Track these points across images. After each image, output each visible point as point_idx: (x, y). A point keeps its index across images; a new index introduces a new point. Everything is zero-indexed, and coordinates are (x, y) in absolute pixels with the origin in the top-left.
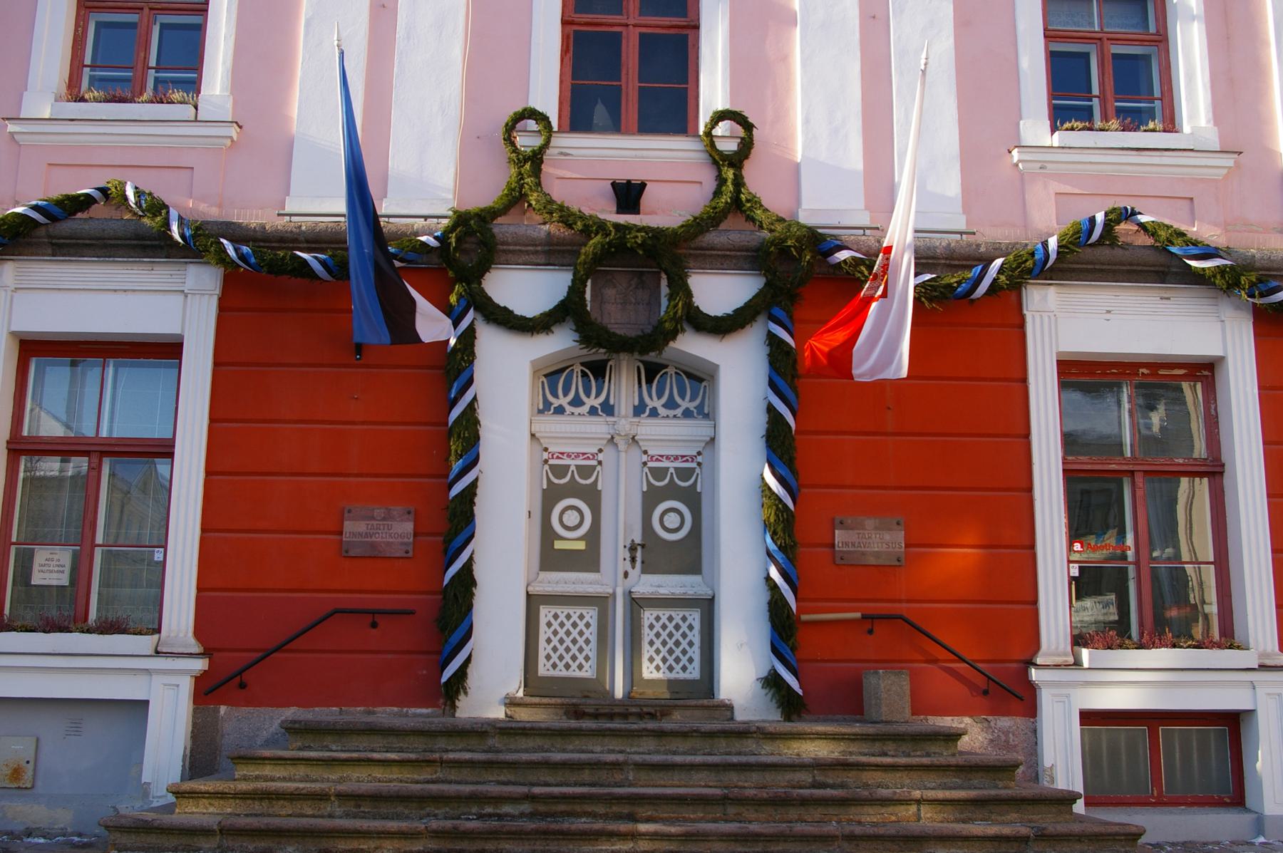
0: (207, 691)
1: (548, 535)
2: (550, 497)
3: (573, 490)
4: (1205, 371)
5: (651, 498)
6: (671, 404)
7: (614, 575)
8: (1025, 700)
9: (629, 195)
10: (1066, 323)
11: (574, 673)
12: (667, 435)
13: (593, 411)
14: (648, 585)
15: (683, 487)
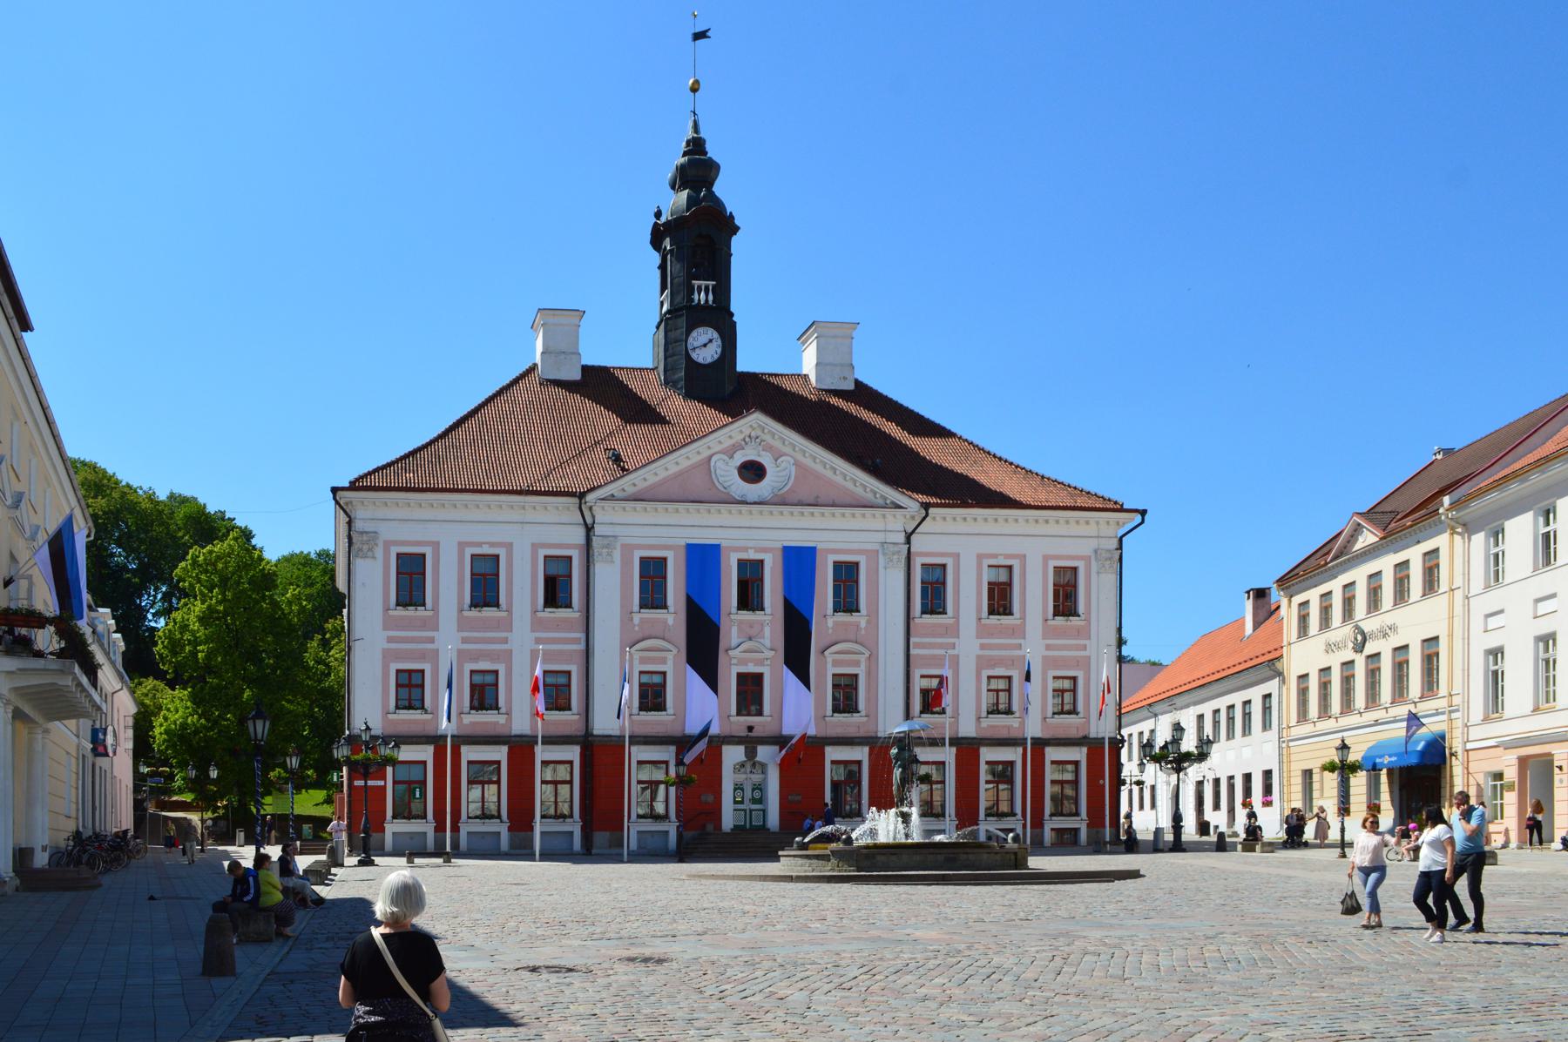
9: (750, 729)
10: (832, 754)
15: (760, 788)
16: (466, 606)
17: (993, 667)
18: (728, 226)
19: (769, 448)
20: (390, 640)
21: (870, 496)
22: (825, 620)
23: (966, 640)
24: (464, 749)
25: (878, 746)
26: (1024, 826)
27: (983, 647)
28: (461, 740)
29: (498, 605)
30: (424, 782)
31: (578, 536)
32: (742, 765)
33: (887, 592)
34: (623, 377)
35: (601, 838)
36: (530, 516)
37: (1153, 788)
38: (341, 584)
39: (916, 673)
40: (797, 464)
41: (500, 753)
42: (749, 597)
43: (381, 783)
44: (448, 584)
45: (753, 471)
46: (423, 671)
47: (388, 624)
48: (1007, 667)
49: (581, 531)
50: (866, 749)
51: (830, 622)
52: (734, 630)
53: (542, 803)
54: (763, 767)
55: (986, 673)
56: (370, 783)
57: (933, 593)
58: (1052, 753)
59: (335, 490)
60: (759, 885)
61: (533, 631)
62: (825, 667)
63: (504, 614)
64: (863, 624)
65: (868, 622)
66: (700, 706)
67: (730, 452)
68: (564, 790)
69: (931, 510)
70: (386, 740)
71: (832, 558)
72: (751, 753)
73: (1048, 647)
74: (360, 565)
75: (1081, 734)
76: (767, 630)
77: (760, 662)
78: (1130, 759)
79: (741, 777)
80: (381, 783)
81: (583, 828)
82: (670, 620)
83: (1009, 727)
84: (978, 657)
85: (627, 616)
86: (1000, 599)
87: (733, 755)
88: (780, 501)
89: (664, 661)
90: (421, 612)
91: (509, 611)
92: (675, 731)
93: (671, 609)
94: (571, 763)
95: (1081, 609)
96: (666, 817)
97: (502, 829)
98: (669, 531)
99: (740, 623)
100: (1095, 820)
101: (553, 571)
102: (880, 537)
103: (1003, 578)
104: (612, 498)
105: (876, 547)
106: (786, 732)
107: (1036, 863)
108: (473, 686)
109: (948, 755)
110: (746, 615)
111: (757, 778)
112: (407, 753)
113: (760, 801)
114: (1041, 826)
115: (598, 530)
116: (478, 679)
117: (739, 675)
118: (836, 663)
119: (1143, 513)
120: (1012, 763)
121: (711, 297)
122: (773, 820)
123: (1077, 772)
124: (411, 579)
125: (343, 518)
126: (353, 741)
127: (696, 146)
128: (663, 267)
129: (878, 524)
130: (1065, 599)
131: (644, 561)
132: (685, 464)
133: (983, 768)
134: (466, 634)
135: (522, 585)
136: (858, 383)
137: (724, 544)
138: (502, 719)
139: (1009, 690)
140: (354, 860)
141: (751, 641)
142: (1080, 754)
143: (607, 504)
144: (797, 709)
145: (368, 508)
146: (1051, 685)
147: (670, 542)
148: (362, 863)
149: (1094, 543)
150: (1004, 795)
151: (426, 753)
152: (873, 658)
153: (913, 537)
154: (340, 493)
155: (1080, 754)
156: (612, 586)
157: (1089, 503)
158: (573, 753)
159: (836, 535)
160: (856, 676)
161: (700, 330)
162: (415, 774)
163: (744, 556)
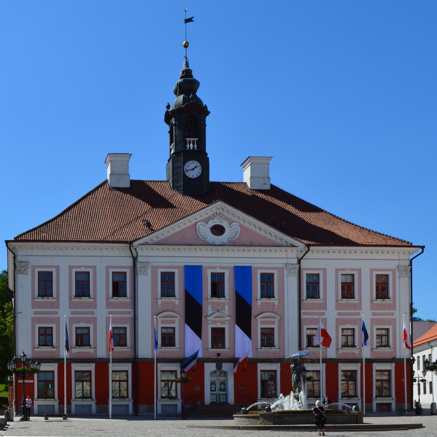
1: (211, 388)
2: (211, 384)
3: (213, 384)
5: (220, 385)
9: (219, 355)
10: (261, 367)
12: (222, 378)
14: (221, 393)
15: (224, 384)
16: (73, 297)
17: (345, 324)
18: (205, 112)
19: (226, 219)
20: (35, 313)
21: (279, 241)
22: (258, 302)
23: (330, 312)
24: (73, 365)
25: (285, 363)
26: (362, 402)
27: (339, 314)
28: (70, 361)
29: (89, 296)
30: (53, 381)
31: (129, 262)
32: (215, 372)
33: (289, 288)
34: (151, 185)
35: (142, 408)
36: (105, 253)
37: (431, 383)
38: (11, 287)
39: (304, 327)
40: (241, 226)
41: (91, 367)
42: (217, 290)
43: (32, 381)
44: (64, 286)
45: (218, 230)
46: (52, 328)
47: (34, 305)
48: (352, 324)
50: (279, 365)
51: (259, 303)
52: (210, 307)
53: (113, 391)
54: (225, 373)
55: (341, 327)
56: (26, 381)
57: (312, 287)
58: (376, 366)
59: (7, 242)
60: (222, 431)
61: (107, 308)
62: (258, 324)
63: (92, 300)
64: (276, 303)
65: (279, 302)
66: (192, 344)
67: (206, 221)
68: (124, 384)
69: (311, 248)
70: (33, 361)
71: (259, 272)
72: (219, 367)
73: (374, 314)
74: (20, 277)
75: (391, 357)
76: (227, 307)
77: (223, 323)
78: (419, 369)
79: (214, 378)
80: (32, 381)
81: (134, 403)
82: (177, 302)
83: (353, 354)
84: (337, 319)
85: (154, 300)
86: (348, 290)
87: (209, 367)
88: (232, 244)
89: (174, 322)
90: (50, 299)
91: (95, 298)
92: (179, 355)
93: (177, 297)
94: (127, 371)
95: (391, 295)
96: (176, 398)
97: (93, 404)
98: (176, 259)
99: (213, 304)
100: (400, 398)
101: (117, 279)
102: (285, 261)
103: (349, 280)
104: (146, 244)
105: (283, 266)
106: (237, 356)
107: (367, 420)
108: (77, 335)
109: (322, 367)
110: (215, 300)
111: (222, 378)
112: (44, 367)
113: (224, 390)
114: (371, 402)
115: (139, 259)
116: (79, 331)
117: (213, 329)
118: (262, 323)
119: (423, 247)
120: (355, 371)
121: (196, 146)
122: (231, 399)
123: (390, 375)
124: (45, 284)
125: (11, 255)
126: (18, 362)
127: (187, 73)
128: (171, 132)
129: (284, 255)
130: (382, 289)
131: (163, 274)
132: (183, 227)
133: (340, 374)
134: (73, 310)
135: (101, 286)
136: (272, 186)
137: (204, 265)
138: (92, 351)
139: (353, 335)
140: (19, 418)
141: (219, 312)
142: (391, 367)
143: (143, 247)
144: (242, 345)
145: (24, 251)
146: (375, 333)
147: (176, 265)
148: (22, 420)
149: (397, 263)
150: (351, 387)
151: (54, 367)
152: (282, 320)
153: (302, 261)
154: (9, 244)
155: (391, 367)
156: (147, 287)
157: (394, 243)
158: (128, 367)
159: (261, 260)
160: (273, 329)
161: (191, 162)
162: (49, 377)
163: (214, 271)
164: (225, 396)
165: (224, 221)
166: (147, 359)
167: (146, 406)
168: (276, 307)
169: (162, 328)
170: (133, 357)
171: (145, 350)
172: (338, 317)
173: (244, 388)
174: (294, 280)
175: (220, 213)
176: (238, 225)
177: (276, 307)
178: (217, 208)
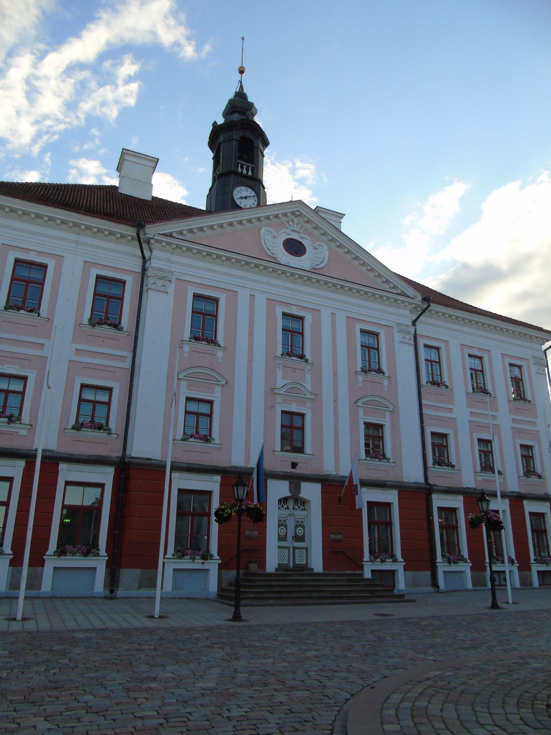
0: (221, 567)
2: (279, 525)
4: (388, 505)
5: (296, 527)
6: (299, 508)
7: (290, 542)
8: (361, 567)
11: (283, 562)
12: (300, 514)
13: (285, 509)
14: (297, 544)
49: (140, 262)
55: (476, 436)
61: (73, 342)
72: (295, 488)
85: (177, 344)
87: (278, 489)
104: (170, 235)
113: (301, 539)
135: (68, 297)
152: (394, 412)
153: (417, 324)
158: (106, 476)
164: (304, 551)
165: (303, 236)
166: (150, 459)
167: (138, 571)
168: (386, 389)
169: (188, 399)
170: (120, 454)
171: (149, 441)
172: (471, 419)
173: (340, 537)
174: (411, 349)
175: (298, 224)
176: (326, 248)
177: (386, 389)
178: (293, 213)
